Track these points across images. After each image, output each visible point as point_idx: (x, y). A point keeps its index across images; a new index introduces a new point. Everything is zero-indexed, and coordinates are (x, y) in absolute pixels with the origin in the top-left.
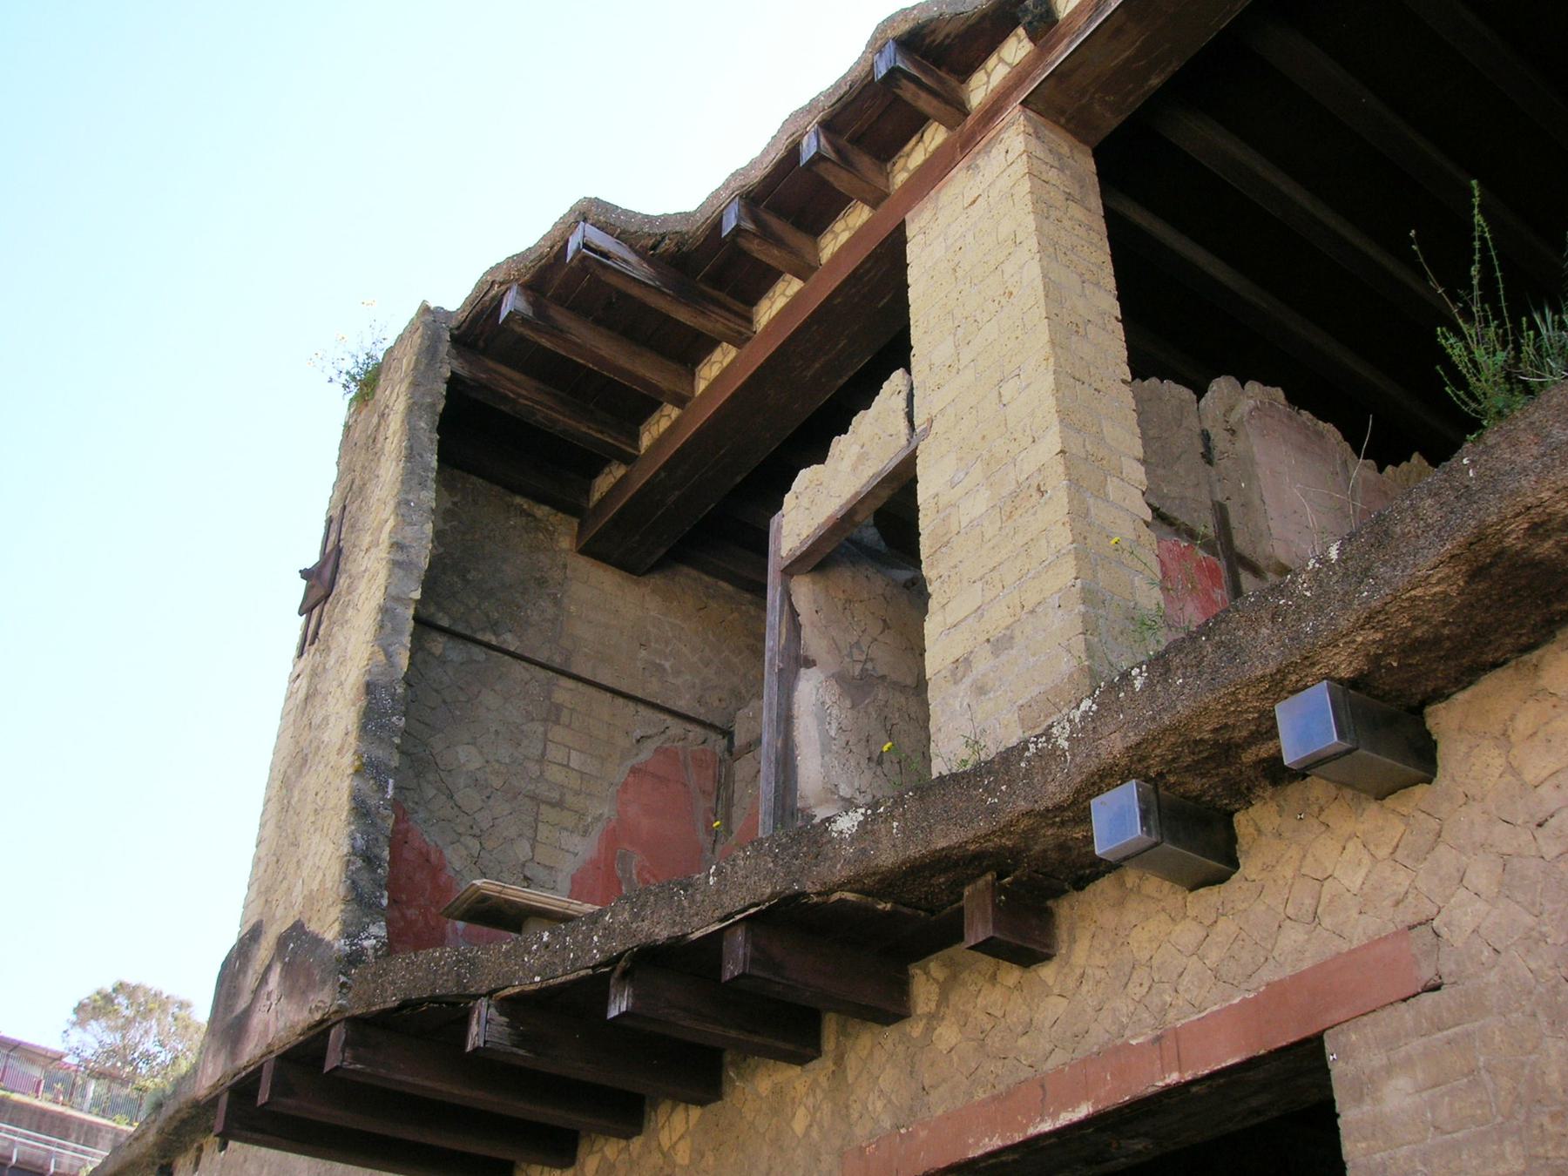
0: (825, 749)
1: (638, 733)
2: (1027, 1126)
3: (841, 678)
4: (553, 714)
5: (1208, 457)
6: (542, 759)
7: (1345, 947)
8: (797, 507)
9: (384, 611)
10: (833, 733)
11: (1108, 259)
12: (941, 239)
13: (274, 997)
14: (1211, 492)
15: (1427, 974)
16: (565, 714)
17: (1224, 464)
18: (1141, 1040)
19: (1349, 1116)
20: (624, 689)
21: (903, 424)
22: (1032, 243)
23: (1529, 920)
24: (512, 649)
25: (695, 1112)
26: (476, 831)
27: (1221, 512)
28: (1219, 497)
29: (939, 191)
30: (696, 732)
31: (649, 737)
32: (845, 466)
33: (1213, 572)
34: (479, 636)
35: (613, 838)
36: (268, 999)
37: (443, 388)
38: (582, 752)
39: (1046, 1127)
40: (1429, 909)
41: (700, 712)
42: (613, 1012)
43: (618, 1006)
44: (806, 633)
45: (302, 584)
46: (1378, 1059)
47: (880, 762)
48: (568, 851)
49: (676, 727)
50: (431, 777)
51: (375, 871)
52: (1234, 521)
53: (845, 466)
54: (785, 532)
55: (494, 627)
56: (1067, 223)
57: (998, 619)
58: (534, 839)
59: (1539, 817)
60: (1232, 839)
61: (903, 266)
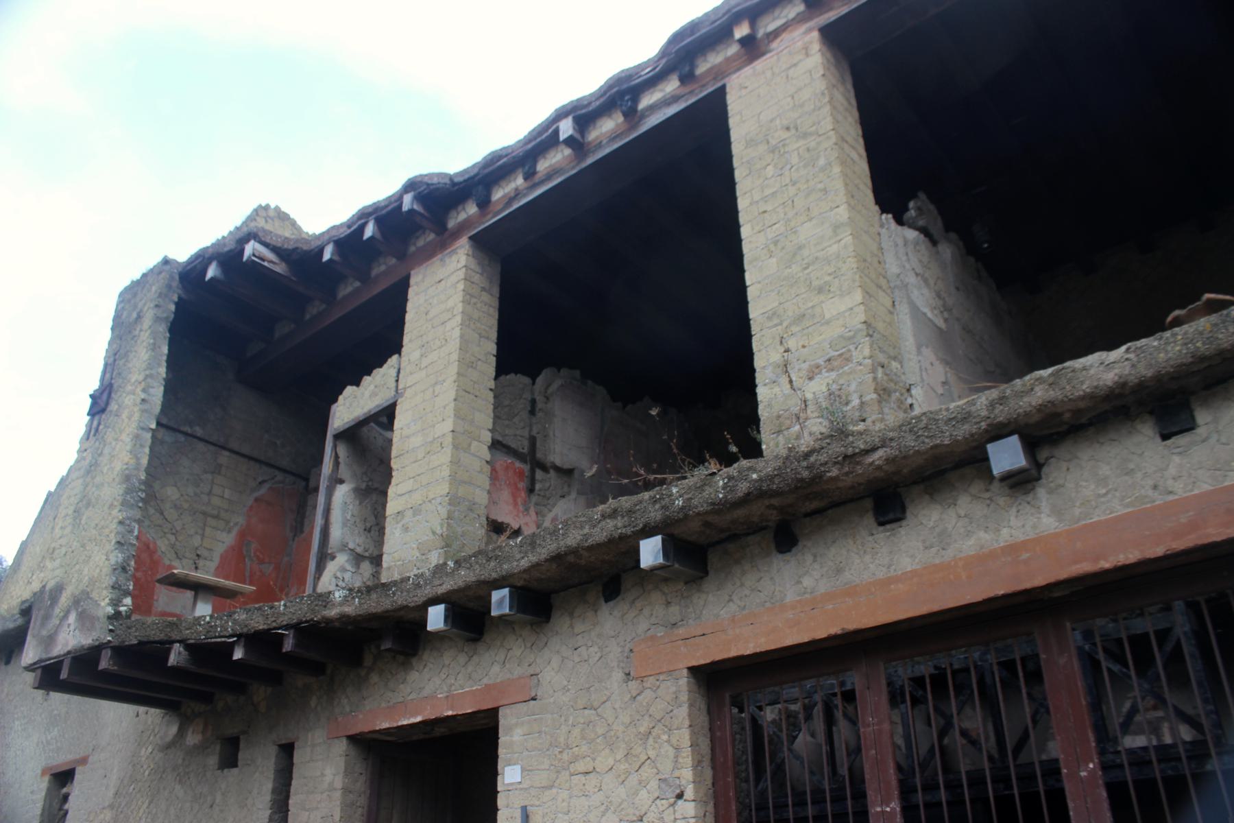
0: (344, 524)
1: (260, 479)
2: (397, 721)
4: (217, 470)
5: (532, 412)
6: (210, 493)
8: (344, 404)
9: (137, 437)
10: (349, 518)
13: (72, 628)
14: (531, 430)
15: (533, 694)
17: (540, 415)
19: (503, 739)
21: (394, 384)
22: (459, 319)
23: (565, 683)
24: (199, 435)
26: (174, 531)
27: (533, 441)
28: (534, 433)
33: (521, 474)
35: (242, 535)
36: (68, 627)
37: (173, 307)
39: (405, 722)
40: (538, 670)
43: (238, 654)
44: (342, 467)
45: (89, 401)
46: (514, 721)
47: (369, 531)
48: (219, 541)
49: (280, 476)
50: (152, 503)
51: (127, 572)
53: (367, 393)
54: (338, 414)
56: (479, 305)
57: (417, 498)
59: (576, 646)
61: (405, 300)
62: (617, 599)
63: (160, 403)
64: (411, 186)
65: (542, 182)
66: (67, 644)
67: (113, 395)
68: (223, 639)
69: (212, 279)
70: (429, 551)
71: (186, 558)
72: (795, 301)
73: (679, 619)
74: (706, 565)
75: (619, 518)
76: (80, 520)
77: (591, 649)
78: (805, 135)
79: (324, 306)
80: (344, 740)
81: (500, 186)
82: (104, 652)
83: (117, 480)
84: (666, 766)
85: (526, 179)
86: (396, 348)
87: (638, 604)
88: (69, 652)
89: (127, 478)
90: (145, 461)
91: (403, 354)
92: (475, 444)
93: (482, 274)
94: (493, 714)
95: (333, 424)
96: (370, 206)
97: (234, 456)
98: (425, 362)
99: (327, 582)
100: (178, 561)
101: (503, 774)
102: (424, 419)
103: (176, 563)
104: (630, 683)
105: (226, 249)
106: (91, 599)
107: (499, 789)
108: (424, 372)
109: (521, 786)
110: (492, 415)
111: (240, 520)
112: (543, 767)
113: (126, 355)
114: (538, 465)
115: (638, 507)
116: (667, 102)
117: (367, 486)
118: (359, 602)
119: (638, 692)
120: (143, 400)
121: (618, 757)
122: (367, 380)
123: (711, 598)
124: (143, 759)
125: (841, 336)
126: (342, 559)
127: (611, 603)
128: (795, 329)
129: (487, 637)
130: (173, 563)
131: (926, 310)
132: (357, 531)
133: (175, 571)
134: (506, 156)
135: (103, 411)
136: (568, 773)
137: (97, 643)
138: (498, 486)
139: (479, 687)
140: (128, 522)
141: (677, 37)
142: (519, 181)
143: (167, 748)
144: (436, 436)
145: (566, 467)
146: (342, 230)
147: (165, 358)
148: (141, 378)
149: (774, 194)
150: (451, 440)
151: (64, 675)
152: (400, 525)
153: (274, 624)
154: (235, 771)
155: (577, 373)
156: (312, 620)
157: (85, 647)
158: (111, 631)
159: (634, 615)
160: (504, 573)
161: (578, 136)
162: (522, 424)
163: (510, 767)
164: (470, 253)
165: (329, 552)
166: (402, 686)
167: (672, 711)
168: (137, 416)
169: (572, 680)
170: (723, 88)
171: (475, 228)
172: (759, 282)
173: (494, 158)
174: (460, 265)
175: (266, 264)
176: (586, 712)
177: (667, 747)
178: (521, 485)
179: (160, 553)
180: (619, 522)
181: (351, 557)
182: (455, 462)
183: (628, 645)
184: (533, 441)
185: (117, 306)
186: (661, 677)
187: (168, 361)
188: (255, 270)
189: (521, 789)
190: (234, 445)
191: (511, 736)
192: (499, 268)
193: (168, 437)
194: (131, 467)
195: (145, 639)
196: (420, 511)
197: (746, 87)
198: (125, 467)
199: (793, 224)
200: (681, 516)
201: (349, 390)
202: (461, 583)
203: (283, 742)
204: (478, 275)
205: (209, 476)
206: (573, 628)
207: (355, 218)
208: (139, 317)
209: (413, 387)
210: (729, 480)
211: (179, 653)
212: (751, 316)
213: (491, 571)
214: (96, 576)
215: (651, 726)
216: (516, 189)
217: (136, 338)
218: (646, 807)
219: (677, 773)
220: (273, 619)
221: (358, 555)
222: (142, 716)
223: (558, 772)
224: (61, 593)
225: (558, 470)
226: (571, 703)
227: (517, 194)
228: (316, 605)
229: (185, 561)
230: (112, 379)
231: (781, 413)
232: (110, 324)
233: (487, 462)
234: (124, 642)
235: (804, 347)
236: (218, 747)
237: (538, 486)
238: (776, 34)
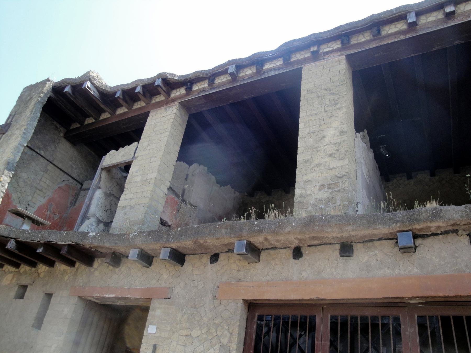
0: (97, 206)
1: (63, 179)
4: (46, 171)
5: (186, 179)
6: (40, 180)
8: (109, 157)
10: (99, 204)
12: (155, 120)
15: (169, 297)
16: (49, 172)
18: (126, 288)
20: (63, 169)
21: (133, 154)
22: (168, 133)
24: (42, 155)
25: (47, 268)
26: (21, 192)
29: (158, 110)
30: (75, 182)
31: (65, 181)
32: (120, 155)
34: (36, 150)
35: (50, 200)
38: (49, 180)
39: (107, 296)
40: (173, 286)
41: (77, 178)
42: (38, 251)
43: (40, 250)
44: (102, 182)
47: (106, 211)
49: (71, 180)
53: (120, 155)
54: (105, 160)
55: (40, 149)
56: (177, 130)
58: (33, 196)
59: (193, 280)
60: (152, 261)
61: (146, 121)
67: (10, 128)
69: (66, 92)
71: (23, 204)
74: (259, 257)
77: (200, 282)
78: (333, 94)
79: (110, 116)
80: (77, 297)
85: (209, 85)
90: (18, 159)
91: (140, 142)
92: (163, 185)
93: (181, 118)
94: (149, 300)
95: (102, 163)
99: (84, 228)
100: (19, 204)
103: (18, 205)
104: (215, 301)
107: (144, 334)
109: (155, 335)
110: (172, 176)
111: (50, 194)
113: (20, 113)
114: (184, 201)
116: (275, 69)
117: (110, 192)
120: (24, 133)
122: (121, 149)
125: (336, 176)
128: (316, 168)
130: (17, 205)
131: (365, 175)
132: (101, 210)
133: (18, 208)
136: (178, 334)
139: (145, 288)
141: (286, 44)
142: (205, 84)
144: (147, 179)
145: (194, 205)
147: (38, 119)
149: (316, 114)
150: (154, 181)
154: (22, 300)
155: (206, 168)
161: (235, 73)
163: (151, 326)
164: (178, 109)
165: (88, 216)
170: (302, 68)
174: (173, 113)
177: (226, 332)
179: (12, 199)
181: (96, 220)
185: (22, 93)
188: (85, 94)
189: (155, 336)
193: (29, 152)
194: (11, 159)
196: (134, 207)
197: (311, 71)
198: (8, 159)
199: (322, 127)
201: (113, 151)
203: (48, 292)
204: (179, 118)
205: (42, 173)
208: (31, 99)
212: (297, 160)
215: (221, 321)
216: (204, 88)
217: (27, 108)
219: (229, 345)
221: (99, 220)
223: (173, 333)
227: (204, 90)
229: (22, 205)
230: (11, 121)
232: (17, 99)
233: (166, 194)
235: (319, 177)
238: (328, 53)
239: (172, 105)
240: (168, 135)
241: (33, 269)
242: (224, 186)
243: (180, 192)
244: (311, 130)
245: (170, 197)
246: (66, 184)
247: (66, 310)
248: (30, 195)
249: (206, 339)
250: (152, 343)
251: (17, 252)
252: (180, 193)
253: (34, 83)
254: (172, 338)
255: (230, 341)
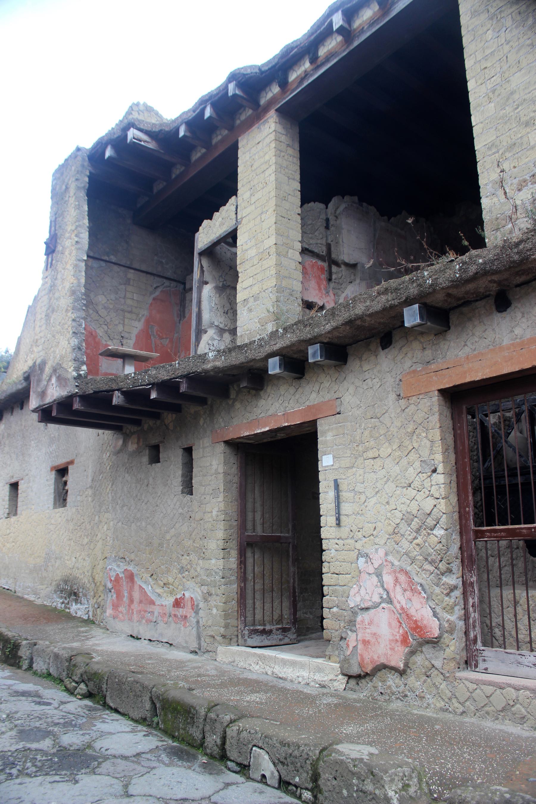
0: (211, 310)
1: (155, 286)
2: (254, 431)
3: (217, 288)
4: (127, 282)
5: (327, 227)
7: (324, 400)
9: (76, 266)
10: (213, 306)
11: (298, 168)
13: (54, 386)
14: (327, 240)
15: (338, 410)
16: (131, 281)
17: (332, 229)
19: (320, 439)
20: (150, 271)
21: (234, 216)
22: (273, 167)
23: (359, 402)
24: (113, 261)
25: (174, 416)
26: (106, 323)
27: (329, 246)
28: (329, 241)
29: (249, 133)
30: (173, 284)
33: (322, 269)
34: (103, 258)
35: (148, 322)
37: (87, 179)
39: (259, 431)
40: (340, 396)
42: (152, 397)
43: (153, 395)
44: (206, 273)
45: (45, 246)
46: (327, 428)
47: (227, 313)
49: (167, 283)
51: (81, 350)
52: (332, 249)
53: (217, 224)
54: (200, 239)
56: (286, 157)
57: (256, 289)
62: (390, 347)
63: (87, 242)
64: (233, 77)
65: (323, 64)
66: (53, 396)
67: (58, 241)
68: (143, 387)
69: (109, 157)
70: (266, 323)
72: (508, 134)
73: (432, 358)
74: (449, 323)
75: (389, 294)
76: (50, 321)
79: (183, 168)
80: (222, 444)
81: (294, 70)
82: (74, 399)
83: (68, 294)
84: (425, 453)
85: (311, 63)
86: (234, 192)
87: (404, 350)
88: (55, 400)
89: (73, 293)
90: (83, 281)
91: (238, 195)
92: (291, 251)
93: (286, 135)
94: (313, 423)
95: (197, 246)
96: (207, 95)
97: (136, 272)
98: (253, 199)
99: (203, 348)
101: (322, 461)
102: (256, 237)
103: (109, 343)
105: (115, 136)
106: (63, 368)
107: (319, 470)
108: (253, 206)
109: (333, 467)
110: (301, 231)
112: (346, 455)
115: (401, 286)
117: (223, 284)
118: (224, 358)
119: (406, 406)
120: (77, 242)
121: (394, 448)
122: (216, 215)
123: (452, 344)
124: (105, 460)
126: (211, 332)
127: (386, 350)
128: (508, 155)
129: (307, 376)
132: (219, 314)
133: (110, 348)
134: (297, 47)
135: (53, 251)
136: (362, 458)
137: (70, 394)
138: (308, 278)
139: (304, 408)
140: (78, 319)
142: (307, 65)
143: (118, 453)
145: (352, 262)
146: (189, 114)
147: (86, 213)
148: (73, 228)
150: (275, 250)
151: (54, 414)
152: (246, 308)
153: (173, 376)
154: (159, 464)
155: (356, 198)
156: (196, 371)
157: (64, 397)
158: (77, 386)
159: (401, 357)
160: (316, 334)
162: (321, 236)
164: (277, 121)
166: (255, 409)
167: (428, 418)
168: (74, 253)
169: (363, 400)
171: (279, 103)
172: (482, 123)
173: (288, 50)
174: (271, 131)
175: (142, 143)
176: (373, 420)
177: (425, 441)
178: (323, 276)
179: (99, 337)
180: (390, 297)
181: (217, 331)
182: (278, 264)
183: (398, 377)
184: (329, 246)
186: (421, 397)
187: (88, 215)
190: (136, 265)
191: (326, 437)
192: (298, 130)
193: (95, 264)
195: (97, 390)
196: (259, 298)
198: (72, 285)
200: (431, 290)
201: (206, 222)
202: (288, 343)
203: (186, 447)
204: (284, 136)
205: (123, 287)
206: (362, 367)
207: (198, 105)
208: (67, 188)
209: (247, 217)
210: (463, 264)
211: (118, 397)
212: (476, 149)
213: (307, 333)
214: (64, 354)
216: (305, 71)
217: (67, 203)
218: (413, 478)
219: (432, 457)
220: (173, 372)
222: (101, 435)
224: (45, 365)
225: (347, 265)
226: (363, 415)
227: (306, 75)
228: (198, 362)
229: (115, 341)
230: (55, 230)
231: (499, 215)
232: (50, 195)
233: (300, 263)
234: (85, 392)
235: (515, 167)
236: (147, 451)
237: (334, 277)
239: (266, 118)
240: (274, 170)
241: (158, 422)
242: (395, 216)
243: (322, 250)
244: (489, 88)
245: (309, 264)
246: (162, 291)
247: (215, 463)
248: (119, 323)
249: (401, 458)
250: (332, 477)
251: (127, 405)
252: (325, 252)
253: (62, 162)
254: (355, 466)
255: (432, 452)
